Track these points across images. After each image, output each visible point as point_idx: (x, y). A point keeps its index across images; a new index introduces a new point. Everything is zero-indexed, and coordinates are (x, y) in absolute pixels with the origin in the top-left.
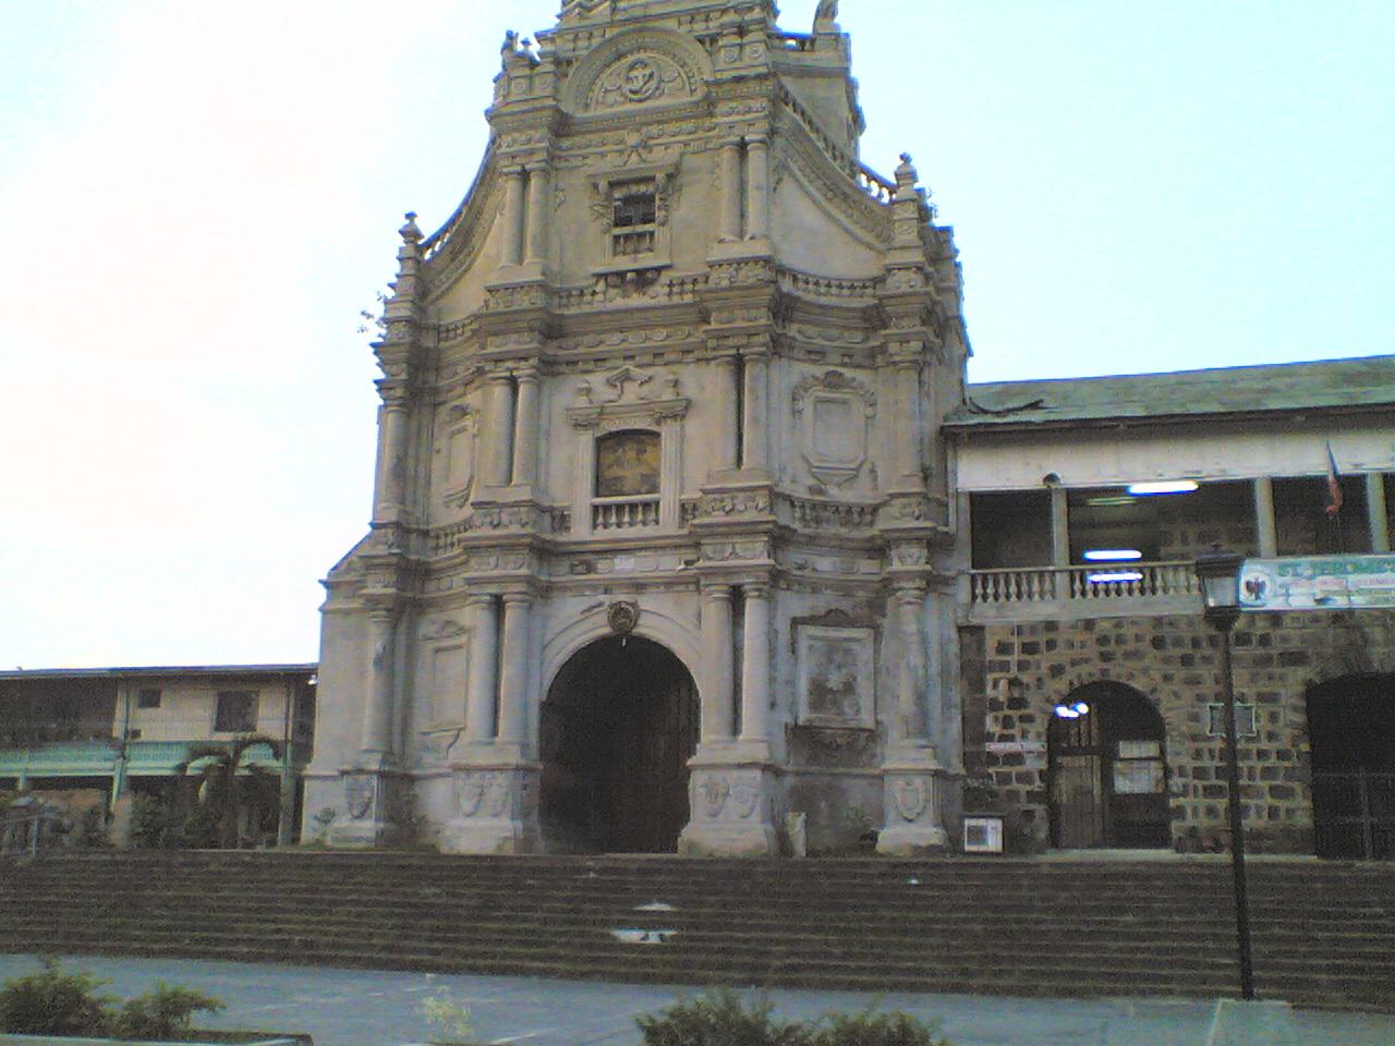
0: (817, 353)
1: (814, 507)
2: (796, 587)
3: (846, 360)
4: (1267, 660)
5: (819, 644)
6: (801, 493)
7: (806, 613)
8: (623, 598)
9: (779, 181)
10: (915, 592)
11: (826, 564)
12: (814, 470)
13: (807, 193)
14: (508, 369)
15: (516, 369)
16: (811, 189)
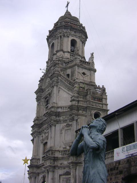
0: (65, 121)
1: (64, 151)
2: (60, 168)
3: (70, 121)
4: (117, 174)
5: (65, 179)
6: (62, 149)
7: (62, 173)
8: (44, 174)
9: (59, 91)
10: (71, 166)
11: (65, 163)
12: (64, 144)
13: (65, 91)
14: (35, 135)
15: (35, 135)
16: (65, 90)
